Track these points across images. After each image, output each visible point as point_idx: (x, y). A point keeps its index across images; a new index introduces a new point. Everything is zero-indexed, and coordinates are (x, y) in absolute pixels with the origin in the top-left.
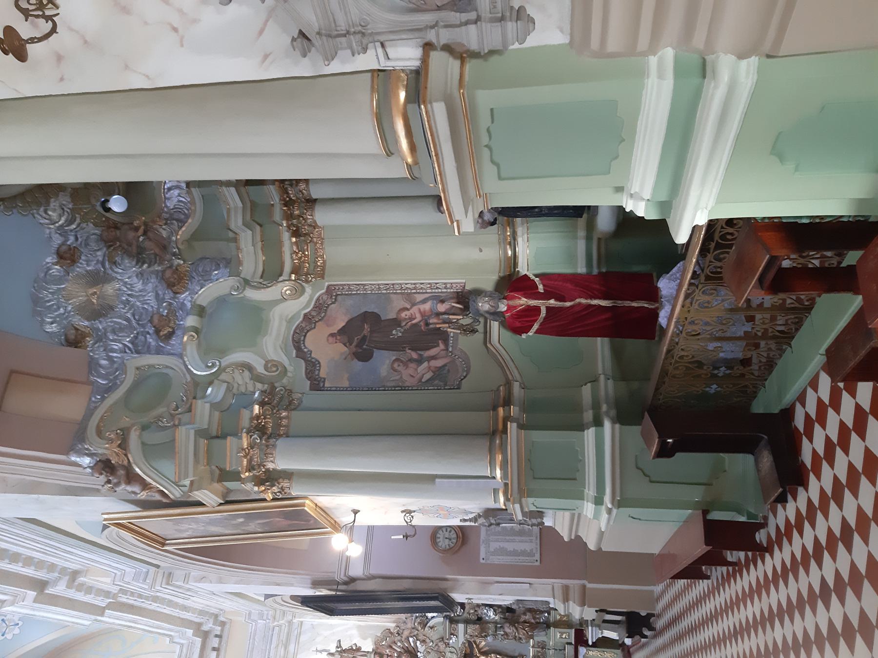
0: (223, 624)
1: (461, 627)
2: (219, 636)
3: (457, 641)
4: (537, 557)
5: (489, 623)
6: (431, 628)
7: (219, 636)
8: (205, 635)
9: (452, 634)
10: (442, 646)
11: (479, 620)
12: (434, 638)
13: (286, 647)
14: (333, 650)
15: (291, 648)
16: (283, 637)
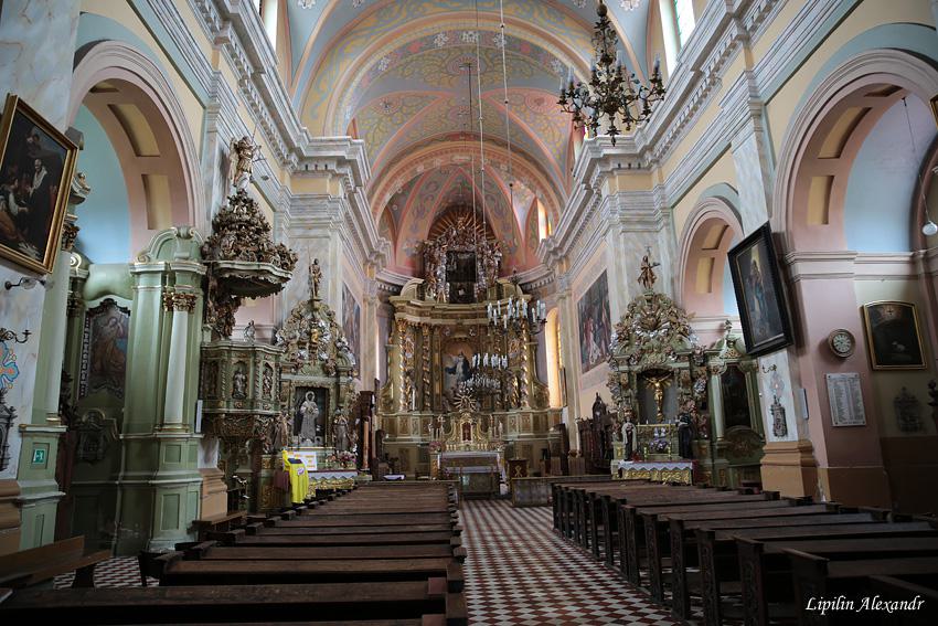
0: (649, 168)
1: (687, 364)
2: (639, 168)
3: (672, 362)
4: (840, 424)
5: (692, 387)
6: (681, 340)
7: (639, 168)
8: (641, 155)
9: (679, 357)
10: (668, 349)
11: (693, 380)
12: (671, 343)
13: (639, 222)
14: (650, 261)
15: (639, 227)
16: (647, 219)
